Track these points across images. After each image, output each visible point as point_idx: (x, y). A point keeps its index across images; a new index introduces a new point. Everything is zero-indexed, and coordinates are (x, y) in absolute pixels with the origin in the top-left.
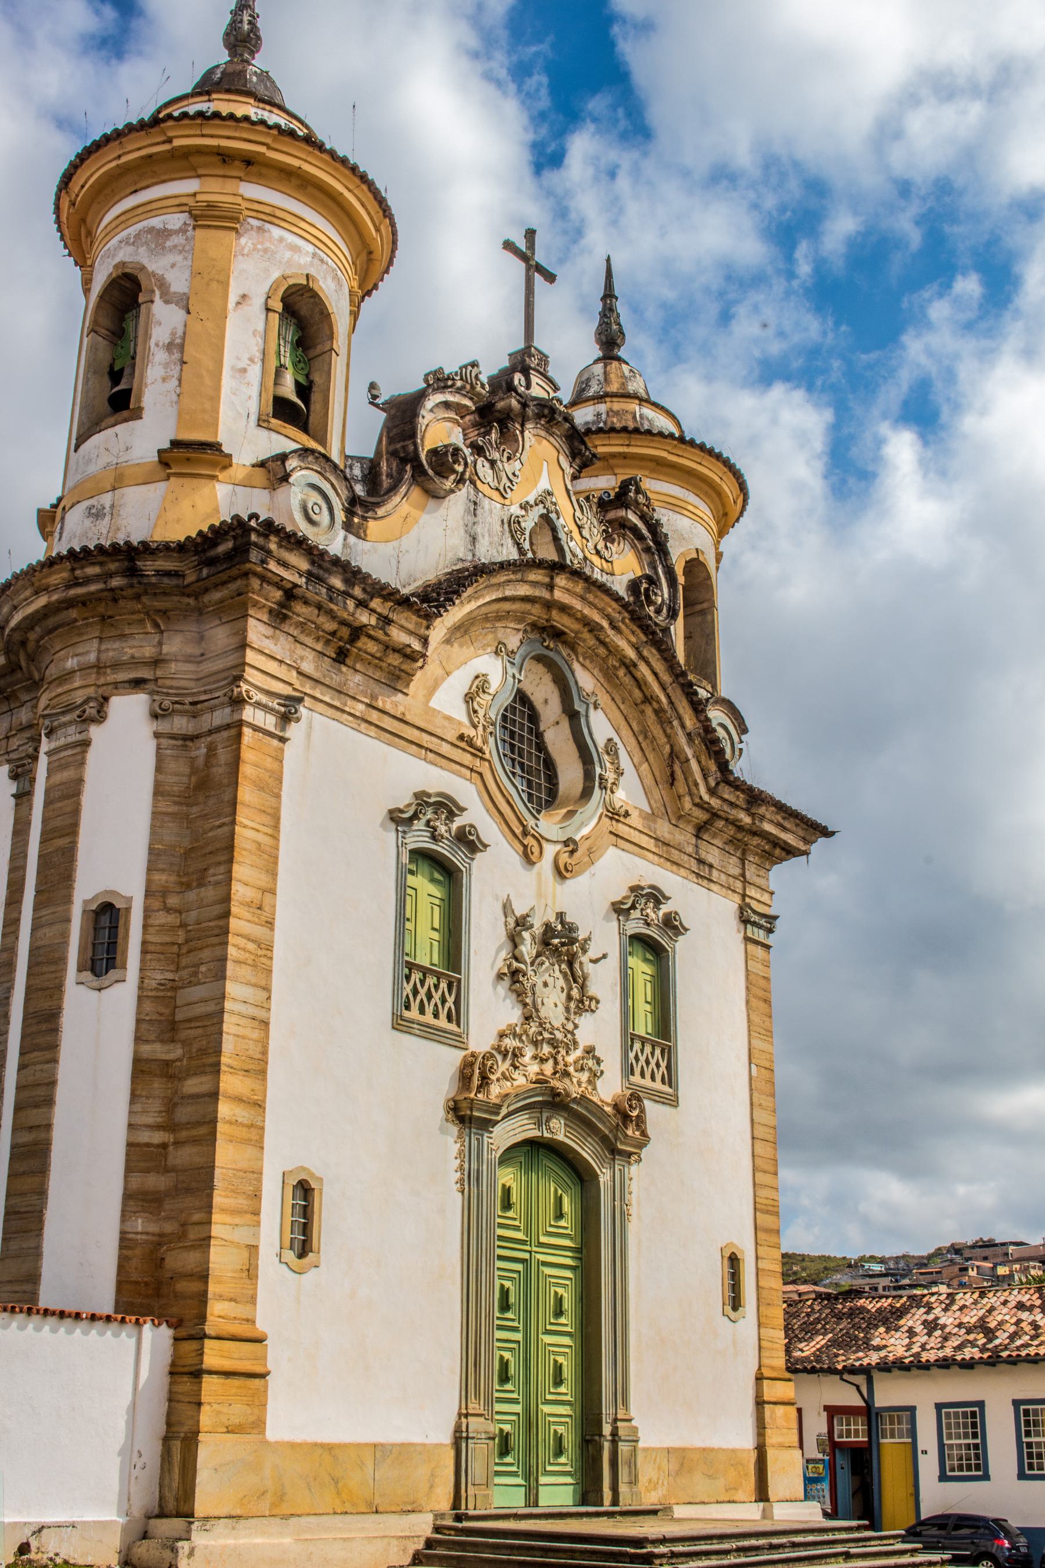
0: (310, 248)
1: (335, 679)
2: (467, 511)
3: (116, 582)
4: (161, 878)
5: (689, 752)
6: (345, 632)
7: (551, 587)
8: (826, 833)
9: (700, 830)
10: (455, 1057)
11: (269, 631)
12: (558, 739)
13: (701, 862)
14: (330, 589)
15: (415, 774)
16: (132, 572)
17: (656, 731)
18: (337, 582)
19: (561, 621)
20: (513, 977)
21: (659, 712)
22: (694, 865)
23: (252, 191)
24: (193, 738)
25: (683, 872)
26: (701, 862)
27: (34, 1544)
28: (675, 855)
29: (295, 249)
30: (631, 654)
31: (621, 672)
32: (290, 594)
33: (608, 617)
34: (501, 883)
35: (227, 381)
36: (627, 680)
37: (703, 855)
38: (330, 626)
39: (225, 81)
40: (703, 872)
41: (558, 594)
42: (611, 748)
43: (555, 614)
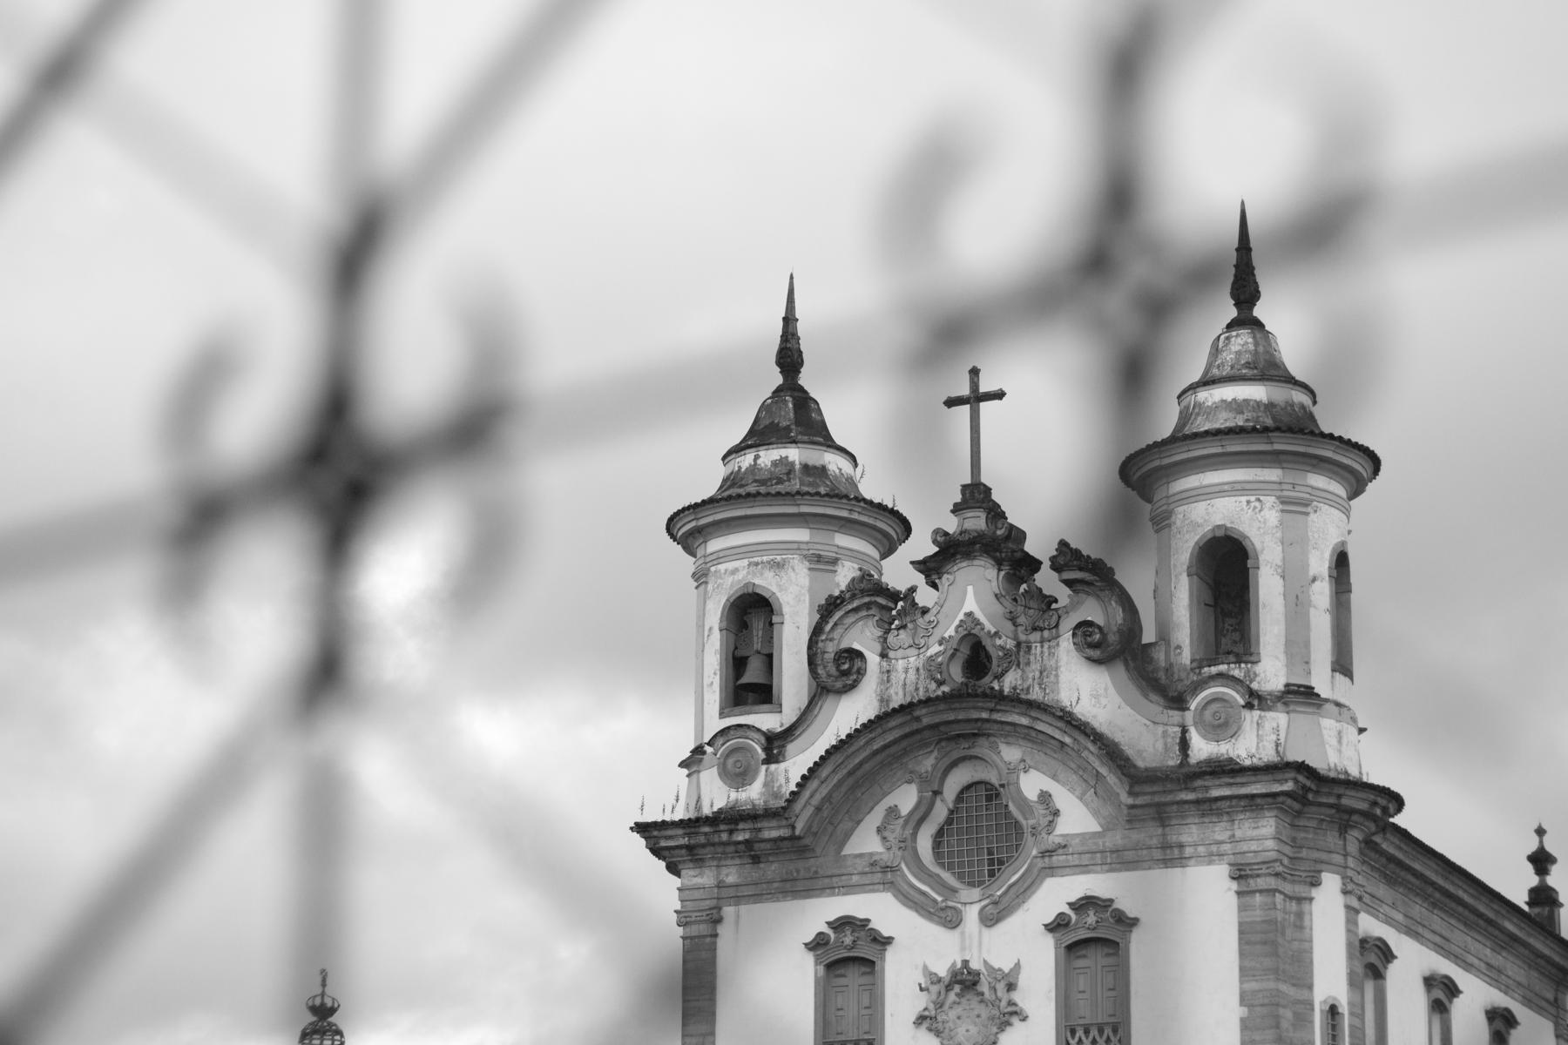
0: (746, 562)
2: (882, 682)
5: (1103, 771)
6: (742, 847)
7: (918, 719)
11: (697, 871)
13: (1165, 847)
18: (707, 829)
22: (1158, 854)
25: (1145, 865)
28: (1130, 855)
30: (1024, 721)
31: (1033, 734)
32: (690, 848)
37: (1174, 839)
40: (1172, 856)
41: (926, 721)
42: (1045, 797)
43: (942, 728)
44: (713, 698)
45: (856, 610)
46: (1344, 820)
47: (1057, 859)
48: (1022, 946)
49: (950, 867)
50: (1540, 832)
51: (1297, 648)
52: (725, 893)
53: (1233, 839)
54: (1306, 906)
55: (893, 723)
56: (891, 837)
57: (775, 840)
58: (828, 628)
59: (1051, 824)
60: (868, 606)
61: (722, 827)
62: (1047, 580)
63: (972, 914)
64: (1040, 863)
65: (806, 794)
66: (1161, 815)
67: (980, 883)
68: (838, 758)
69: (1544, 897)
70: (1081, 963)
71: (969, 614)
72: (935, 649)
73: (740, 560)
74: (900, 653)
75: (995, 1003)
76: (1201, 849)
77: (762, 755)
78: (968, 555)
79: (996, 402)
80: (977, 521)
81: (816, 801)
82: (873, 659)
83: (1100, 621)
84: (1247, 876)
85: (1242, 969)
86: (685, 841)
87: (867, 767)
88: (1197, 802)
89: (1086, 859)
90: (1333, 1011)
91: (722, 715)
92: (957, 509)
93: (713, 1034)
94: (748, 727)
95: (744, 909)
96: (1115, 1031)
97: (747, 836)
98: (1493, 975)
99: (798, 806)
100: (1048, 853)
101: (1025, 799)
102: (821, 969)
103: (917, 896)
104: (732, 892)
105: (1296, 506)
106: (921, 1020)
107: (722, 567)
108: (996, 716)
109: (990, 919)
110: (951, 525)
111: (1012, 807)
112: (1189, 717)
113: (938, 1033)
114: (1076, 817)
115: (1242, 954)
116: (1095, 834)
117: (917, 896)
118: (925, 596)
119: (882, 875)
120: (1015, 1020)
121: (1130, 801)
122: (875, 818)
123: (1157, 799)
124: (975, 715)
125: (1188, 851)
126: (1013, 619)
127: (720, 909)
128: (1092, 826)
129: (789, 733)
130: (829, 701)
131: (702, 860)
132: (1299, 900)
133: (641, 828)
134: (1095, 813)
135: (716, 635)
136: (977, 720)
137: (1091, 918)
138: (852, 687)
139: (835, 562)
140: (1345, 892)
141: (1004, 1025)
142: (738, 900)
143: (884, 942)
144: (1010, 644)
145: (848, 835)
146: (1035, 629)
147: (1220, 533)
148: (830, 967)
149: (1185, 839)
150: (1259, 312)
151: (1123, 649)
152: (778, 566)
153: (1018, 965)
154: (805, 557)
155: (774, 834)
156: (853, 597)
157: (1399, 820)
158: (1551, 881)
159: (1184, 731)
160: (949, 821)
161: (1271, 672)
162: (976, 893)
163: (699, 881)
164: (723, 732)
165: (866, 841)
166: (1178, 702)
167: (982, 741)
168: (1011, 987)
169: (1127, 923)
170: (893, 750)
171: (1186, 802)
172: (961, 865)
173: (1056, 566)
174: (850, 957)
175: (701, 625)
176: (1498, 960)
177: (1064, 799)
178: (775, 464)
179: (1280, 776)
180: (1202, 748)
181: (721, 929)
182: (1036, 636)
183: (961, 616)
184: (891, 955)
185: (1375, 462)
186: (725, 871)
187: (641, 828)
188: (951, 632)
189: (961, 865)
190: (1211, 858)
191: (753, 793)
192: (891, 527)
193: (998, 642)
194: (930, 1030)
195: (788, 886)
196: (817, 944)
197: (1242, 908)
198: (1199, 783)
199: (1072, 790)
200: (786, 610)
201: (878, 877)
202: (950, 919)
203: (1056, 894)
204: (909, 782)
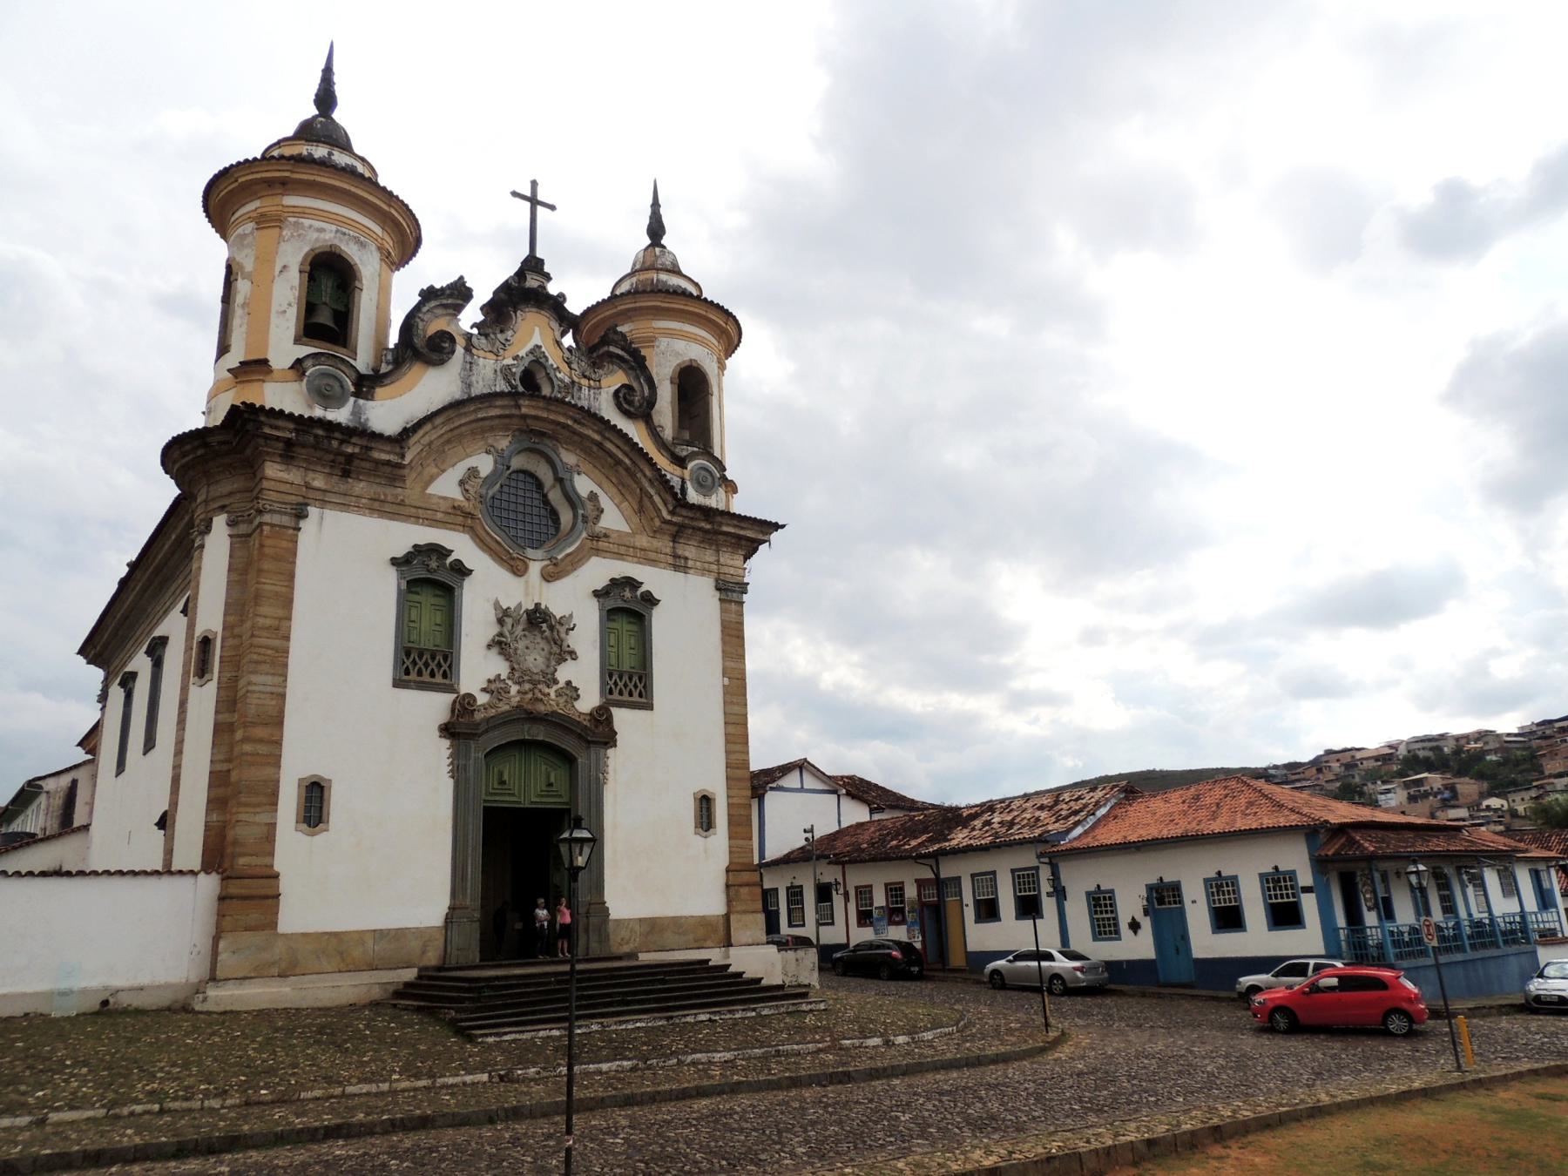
0: (334, 228)
1: (343, 488)
2: (464, 369)
3: (200, 452)
4: (231, 619)
5: (652, 492)
6: (341, 459)
7: (519, 407)
8: (777, 527)
9: (675, 538)
10: (445, 699)
11: (283, 467)
12: (555, 496)
13: (676, 556)
14: (316, 436)
15: (406, 536)
16: (206, 445)
17: (628, 480)
18: (320, 432)
19: (536, 426)
20: (499, 644)
21: (627, 469)
22: (670, 560)
23: (291, 200)
24: (249, 535)
26: (676, 556)
27: (112, 1000)
28: (652, 555)
29: (321, 230)
30: (597, 437)
31: (595, 449)
32: (289, 443)
33: (571, 418)
34: (489, 591)
35: (274, 320)
36: (601, 453)
37: (680, 552)
38: (331, 457)
39: (306, 132)
40: (679, 564)
41: (524, 410)
42: (593, 497)
43: (529, 421)
47: (602, 545)
52: (311, 494)
53: (718, 562)
55: (499, 403)
56: (472, 491)
57: (378, 462)
58: (425, 309)
59: (598, 518)
61: (337, 435)
66: (678, 534)
68: (451, 413)
70: (611, 625)
72: (509, 361)
73: (320, 224)
74: (481, 353)
77: (352, 389)
84: (726, 590)
86: (288, 435)
87: (463, 429)
88: (706, 531)
89: (623, 550)
91: (297, 341)
93: (289, 619)
95: (330, 515)
97: (357, 450)
100: (595, 537)
101: (579, 496)
102: (404, 586)
103: (493, 545)
104: (319, 495)
107: (307, 222)
108: (576, 426)
109: (548, 577)
112: (687, 474)
113: (508, 658)
114: (613, 519)
117: (493, 545)
119: (458, 517)
124: (562, 420)
125: (690, 563)
130: (417, 368)
131: (292, 458)
136: (559, 423)
138: (441, 362)
142: (323, 504)
143: (461, 571)
144: (567, 380)
145: (432, 479)
149: (687, 554)
152: (362, 245)
154: (379, 249)
155: (384, 457)
156: (451, 296)
162: (539, 554)
163: (284, 476)
165: (447, 486)
167: (547, 441)
169: (650, 600)
170: (487, 423)
171: (700, 529)
181: (302, 524)
182: (584, 382)
183: (530, 346)
184: (468, 583)
186: (311, 475)
190: (704, 572)
191: (341, 415)
195: (376, 505)
197: (723, 611)
198: (719, 519)
201: (460, 519)
202: (517, 568)
203: (599, 571)
204: (488, 452)
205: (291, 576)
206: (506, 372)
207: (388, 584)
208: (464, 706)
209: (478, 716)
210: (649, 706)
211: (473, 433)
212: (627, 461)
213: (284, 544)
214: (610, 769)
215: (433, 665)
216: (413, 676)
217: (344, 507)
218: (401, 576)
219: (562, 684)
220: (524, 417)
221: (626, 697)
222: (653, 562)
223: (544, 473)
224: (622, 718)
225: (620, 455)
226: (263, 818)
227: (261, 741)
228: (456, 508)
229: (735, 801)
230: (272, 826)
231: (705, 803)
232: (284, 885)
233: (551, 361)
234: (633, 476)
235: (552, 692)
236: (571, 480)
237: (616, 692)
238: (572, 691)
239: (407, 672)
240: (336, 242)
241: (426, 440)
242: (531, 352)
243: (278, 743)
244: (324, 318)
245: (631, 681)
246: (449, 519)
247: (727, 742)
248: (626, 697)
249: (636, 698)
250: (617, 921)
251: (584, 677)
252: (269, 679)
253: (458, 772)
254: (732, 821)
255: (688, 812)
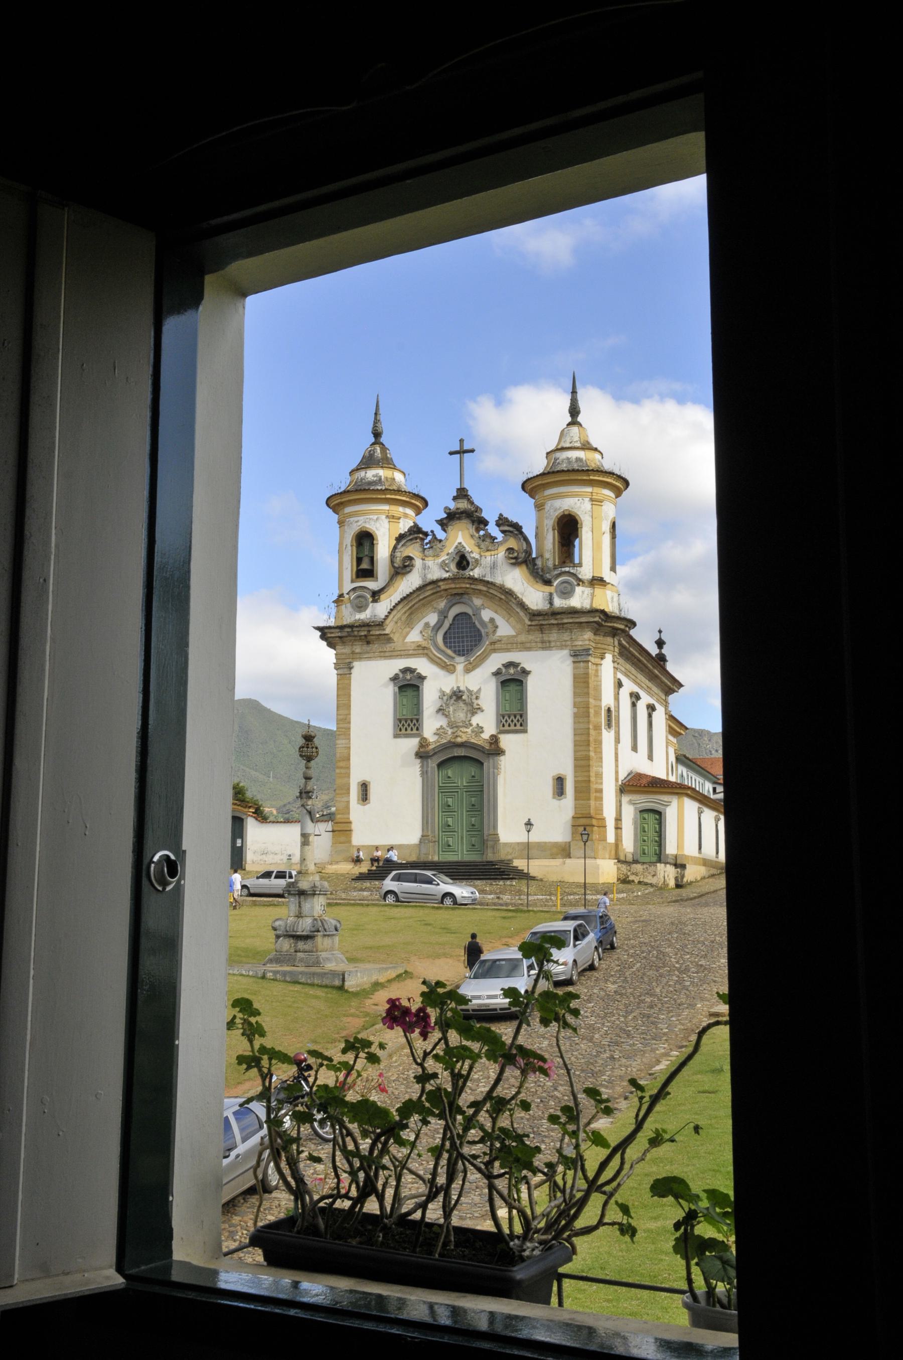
7: (439, 586)
18: (349, 630)
22: (540, 645)
26: (543, 642)
28: (528, 645)
30: (484, 589)
32: (340, 637)
34: (436, 683)
37: (546, 639)
40: (546, 646)
41: (443, 587)
42: (492, 620)
44: (348, 574)
45: (411, 540)
46: (614, 632)
47: (497, 646)
48: (481, 681)
49: (450, 648)
50: (660, 632)
51: (596, 561)
54: (599, 667)
55: (428, 588)
58: (399, 546)
59: (494, 632)
60: (416, 538)
62: (493, 530)
63: (460, 668)
64: (490, 647)
65: (391, 616)
66: (541, 628)
67: (463, 655)
69: (662, 658)
71: (460, 543)
74: (430, 558)
75: (471, 704)
76: (558, 644)
77: (371, 600)
78: (459, 519)
79: (471, 454)
80: (463, 505)
81: (395, 619)
82: (418, 563)
83: (516, 548)
85: (575, 693)
86: (337, 635)
88: (558, 624)
89: (509, 646)
90: (609, 710)
91: (352, 581)
92: (455, 498)
94: (365, 587)
96: (521, 716)
97: (365, 633)
98: (649, 691)
99: (387, 621)
102: (397, 689)
103: (438, 660)
104: (358, 656)
105: (596, 502)
106: (440, 710)
108: (473, 586)
109: (468, 670)
110: (452, 506)
111: (477, 623)
113: (446, 716)
114: (505, 629)
115: (575, 687)
116: (513, 636)
117: (438, 660)
118: (440, 534)
119: (421, 650)
120: (479, 711)
121: (529, 623)
122: (419, 626)
123: (541, 622)
124: (464, 585)
125: (553, 644)
126: (479, 546)
127: (350, 662)
128: (512, 632)
129: (382, 590)
130: (399, 577)
132: (597, 665)
133: (318, 628)
134: (514, 627)
135: (349, 548)
137: (512, 671)
139: (399, 518)
140: (614, 662)
141: (473, 713)
142: (360, 659)
143: (422, 678)
144: (477, 557)
145: (408, 634)
146: (488, 550)
147: (566, 513)
148: (400, 688)
149: (551, 639)
150: (579, 419)
151: (523, 559)
153: (480, 689)
154: (387, 517)
155: (378, 633)
156: (410, 534)
157: (633, 632)
158: (663, 651)
159: (551, 594)
160: (449, 628)
161: (586, 572)
162: (462, 659)
163: (344, 651)
164: (354, 589)
166: (548, 583)
167: (465, 596)
168: (477, 698)
169: (525, 672)
172: (455, 647)
173: (498, 524)
174: (408, 686)
175: (341, 544)
176: (650, 684)
177: (500, 621)
178: (374, 476)
179: (593, 614)
180: (558, 603)
181: (353, 671)
183: (456, 544)
184: (426, 683)
185: (626, 483)
187: (318, 628)
188: (451, 550)
189: (455, 647)
190: (562, 647)
192: (419, 502)
193: (472, 555)
194: (443, 714)
195: (382, 654)
196: (395, 679)
197: (575, 668)
198: (559, 616)
199: (504, 618)
200: (379, 538)
201: (421, 652)
203: (496, 661)
205: (349, 696)
206: (443, 565)
207: (390, 691)
208: (423, 743)
209: (431, 747)
210: (525, 731)
211: (424, 605)
212: (503, 597)
213: (346, 682)
214: (502, 767)
215: (412, 725)
216: (403, 731)
217: (369, 658)
218: (395, 685)
219: (474, 725)
220: (446, 590)
221: (512, 727)
222: (529, 649)
223: (470, 612)
224: (507, 741)
225: (499, 595)
226: (345, 799)
227: (342, 768)
228: (419, 647)
229: (579, 779)
230: (348, 802)
231: (560, 781)
232: (353, 826)
233: (468, 549)
234: (507, 603)
235: (469, 730)
236: (480, 614)
237: (506, 725)
238: (480, 729)
239: (400, 730)
240: (364, 525)
241: (396, 617)
242: (456, 547)
243: (348, 768)
244: (365, 565)
245: (514, 717)
246: (415, 652)
247: (575, 745)
248: (512, 727)
249: (518, 727)
250: (505, 844)
251: (486, 722)
252: (344, 741)
253: (424, 773)
254: (577, 791)
255: (548, 787)
